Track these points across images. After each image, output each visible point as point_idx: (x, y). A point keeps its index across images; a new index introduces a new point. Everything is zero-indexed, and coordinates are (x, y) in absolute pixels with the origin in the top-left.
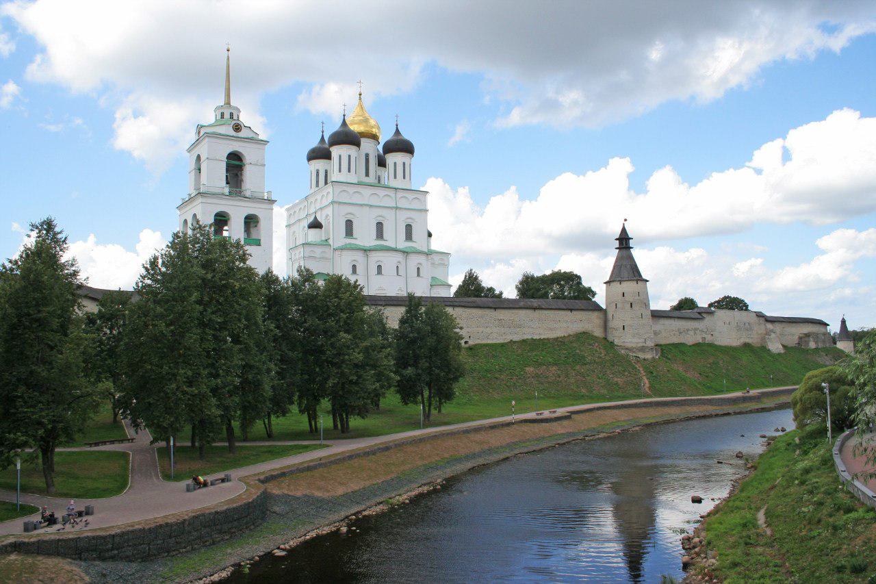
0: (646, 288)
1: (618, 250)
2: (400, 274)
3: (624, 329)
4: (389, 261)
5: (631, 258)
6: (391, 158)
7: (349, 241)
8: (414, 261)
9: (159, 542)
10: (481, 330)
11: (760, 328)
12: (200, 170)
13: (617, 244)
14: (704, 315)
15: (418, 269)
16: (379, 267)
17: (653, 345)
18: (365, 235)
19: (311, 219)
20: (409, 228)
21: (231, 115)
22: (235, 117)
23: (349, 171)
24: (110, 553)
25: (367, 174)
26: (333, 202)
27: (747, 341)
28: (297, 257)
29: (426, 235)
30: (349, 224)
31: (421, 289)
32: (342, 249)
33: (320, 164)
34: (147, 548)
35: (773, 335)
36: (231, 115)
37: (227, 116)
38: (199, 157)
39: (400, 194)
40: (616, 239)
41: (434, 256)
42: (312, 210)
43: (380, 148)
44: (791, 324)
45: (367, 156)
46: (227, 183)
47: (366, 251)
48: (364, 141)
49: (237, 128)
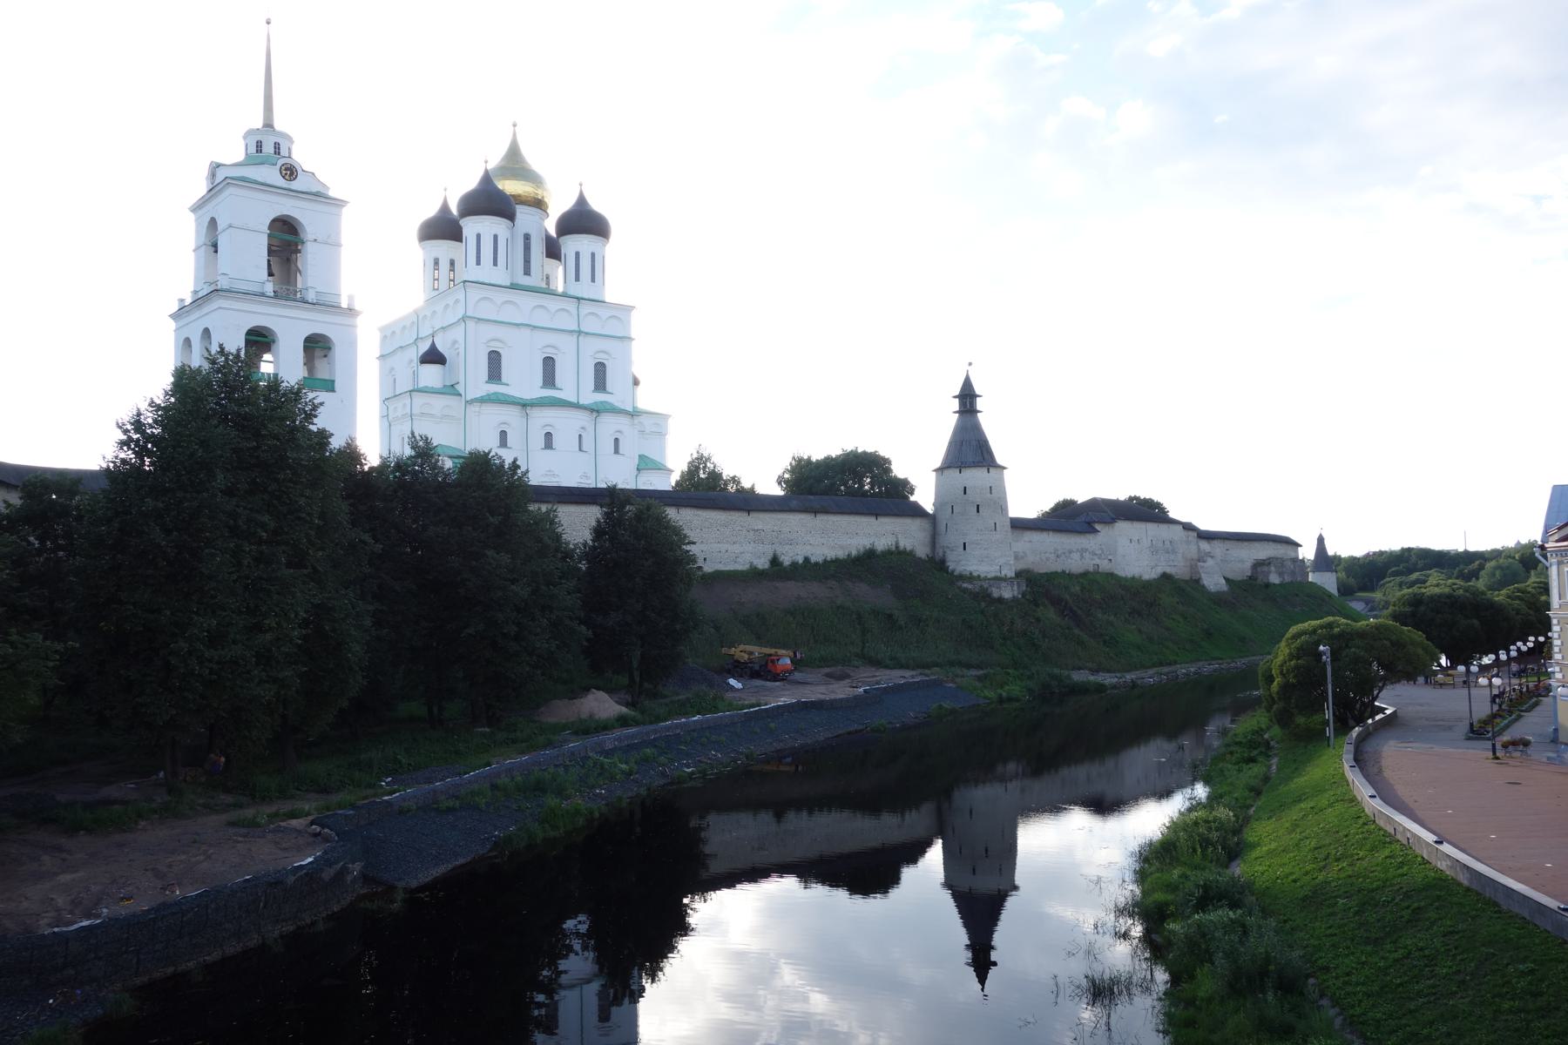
0: (1002, 480)
1: (957, 415)
2: (584, 448)
3: (965, 549)
4: (566, 425)
6: (571, 244)
7: (495, 388)
8: (609, 425)
10: (724, 547)
11: (1194, 548)
12: (215, 246)
13: (956, 405)
14: (1098, 527)
15: (616, 440)
16: (548, 436)
17: (1013, 575)
18: (522, 379)
19: (424, 347)
20: (600, 369)
21: (277, 147)
22: (284, 152)
23: (495, 264)
25: (527, 272)
26: (464, 319)
27: (1168, 570)
28: (399, 414)
29: (631, 381)
30: (495, 359)
31: (620, 475)
32: (482, 400)
33: (444, 249)
34: (135, 961)
35: (1210, 562)
36: (277, 147)
37: (268, 149)
39: (586, 309)
40: (955, 397)
41: (642, 419)
42: (426, 331)
43: (551, 226)
44: (1240, 543)
45: (527, 237)
46: (270, 274)
47: (524, 405)
48: (522, 212)
49: (290, 172)
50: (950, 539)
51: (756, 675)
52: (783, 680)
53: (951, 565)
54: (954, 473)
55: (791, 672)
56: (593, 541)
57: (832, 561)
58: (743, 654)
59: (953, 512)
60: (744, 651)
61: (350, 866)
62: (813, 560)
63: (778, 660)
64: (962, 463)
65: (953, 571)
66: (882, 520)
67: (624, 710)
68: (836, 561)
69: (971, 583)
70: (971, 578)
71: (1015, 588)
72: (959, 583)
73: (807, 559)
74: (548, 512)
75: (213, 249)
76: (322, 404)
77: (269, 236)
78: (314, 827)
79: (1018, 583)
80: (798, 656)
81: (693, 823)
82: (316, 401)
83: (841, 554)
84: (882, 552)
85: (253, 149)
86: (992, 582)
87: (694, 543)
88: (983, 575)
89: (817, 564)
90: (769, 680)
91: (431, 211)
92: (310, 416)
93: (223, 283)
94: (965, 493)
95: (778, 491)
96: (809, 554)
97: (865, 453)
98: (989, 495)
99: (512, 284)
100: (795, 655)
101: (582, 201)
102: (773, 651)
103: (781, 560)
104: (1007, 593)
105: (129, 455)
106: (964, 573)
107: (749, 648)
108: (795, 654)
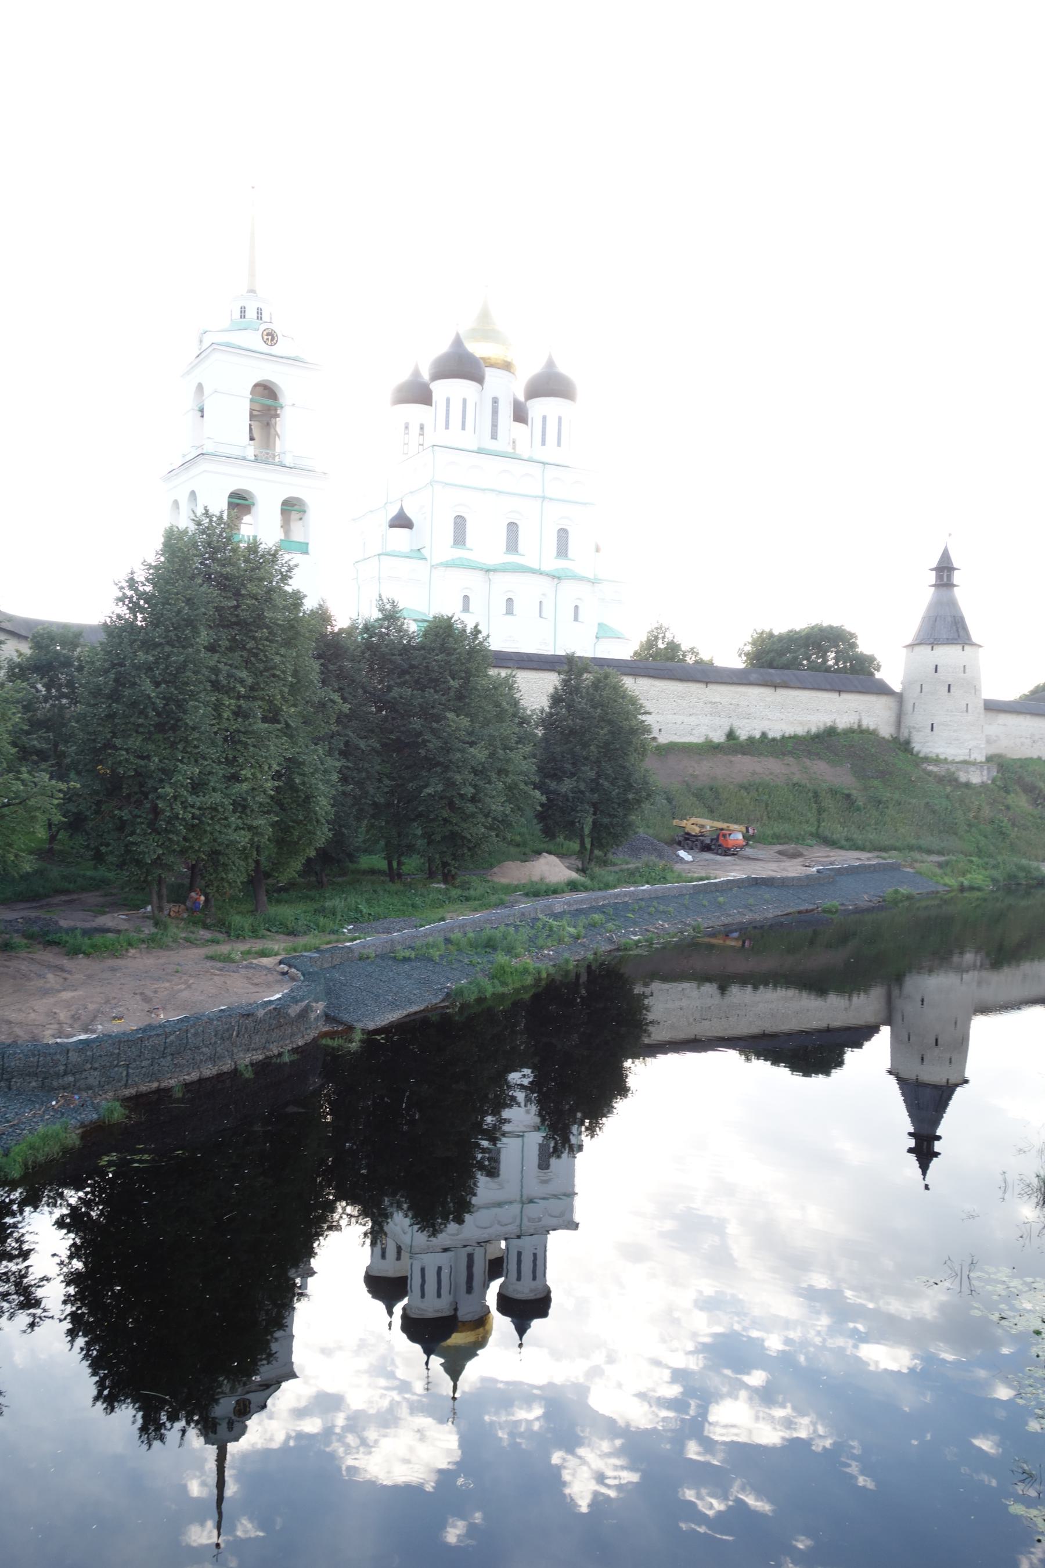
2: (544, 615)
3: (932, 730)
5: (953, 604)
6: (538, 408)
7: (458, 553)
8: (570, 591)
9: (145, 1063)
12: (202, 411)
13: (932, 577)
15: (576, 607)
16: (510, 601)
17: (983, 759)
19: (393, 512)
20: (563, 535)
21: (259, 313)
22: (266, 317)
23: (463, 428)
24: (60, 1081)
25: (494, 436)
26: (431, 483)
30: (460, 523)
32: (447, 565)
34: (125, 1073)
36: (259, 313)
37: (251, 314)
38: (200, 387)
40: (932, 570)
45: (495, 401)
46: (252, 439)
48: (491, 375)
49: (271, 337)
50: (917, 719)
51: (706, 848)
52: (734, 854)
53: (916, 747)
54: (925, 650)
55: (742, 847)
56: (550, 708)
57: (790, 737)
58: (694, 827)
59: (921, 692)
60: (693, 824)
61: (314, 1004)
62: (771, 735)
63: (730, 834)
64: (935, 639)
65: (918, 753)
66: (845, 696)
67: (574, 875)
68: (794, 738)
69: (936, 765)
70: (937, 761)
71: (985, 773)
72: (924, 766)
73: (764, 735)
74: (507, 678)
75: (200, 414)
76: (296, 566)
77: (251, 401)
78: (282, 966)
79: (988, 768)
80: (751, 831)
81: (638, 990)
82: (291, 563)
83: (800, 731)
84: (843, 730)
85: (237, 314)
86: (959, 766)
87: (649, 713)
88: (950, 759)
89: (774, 740)
90: (720, 855)
91: (404, 376)
92: (285, 578)
93: (209, 448)
94: (936, 672)
95: (738, 663)
96: (766, 729)
97: (831, 627)
98: (962, 674)
99: (479, 448)
100: (747, 831)
101: (550, 364)
102: (724, 825)
103: (737, 734)
104: (976, 778)
105: (124, 611)
106: (930, 755)
107: (700, 821)
108: (747, 829)
